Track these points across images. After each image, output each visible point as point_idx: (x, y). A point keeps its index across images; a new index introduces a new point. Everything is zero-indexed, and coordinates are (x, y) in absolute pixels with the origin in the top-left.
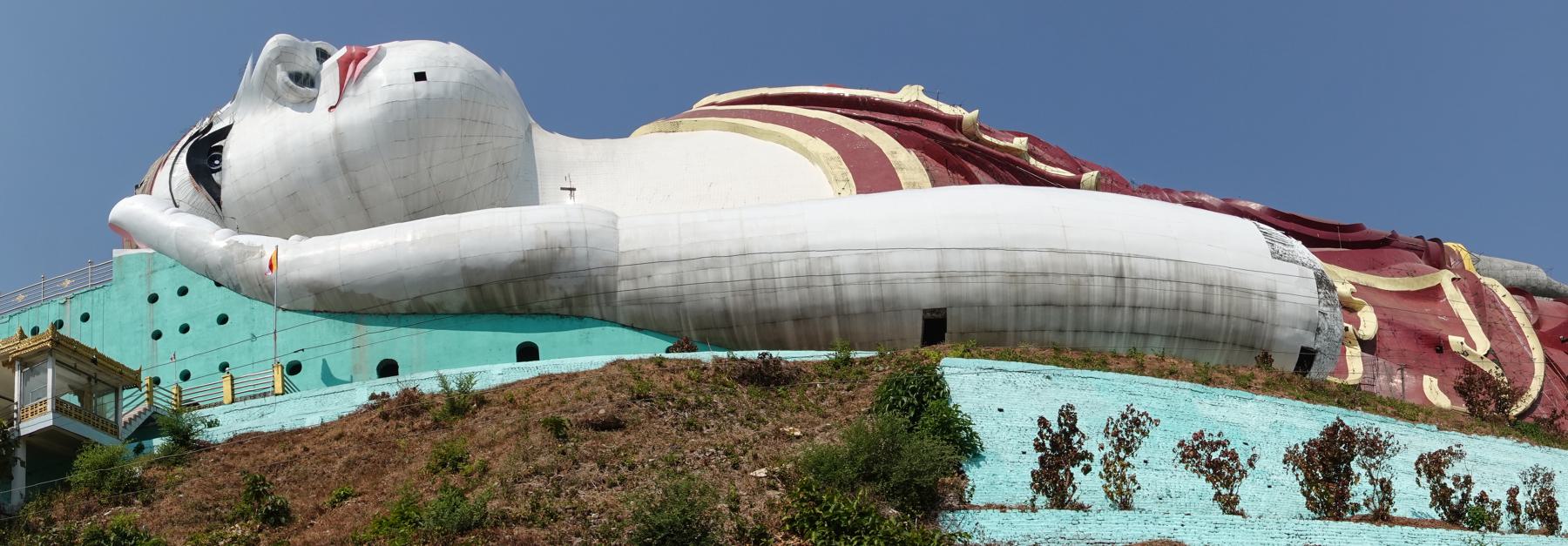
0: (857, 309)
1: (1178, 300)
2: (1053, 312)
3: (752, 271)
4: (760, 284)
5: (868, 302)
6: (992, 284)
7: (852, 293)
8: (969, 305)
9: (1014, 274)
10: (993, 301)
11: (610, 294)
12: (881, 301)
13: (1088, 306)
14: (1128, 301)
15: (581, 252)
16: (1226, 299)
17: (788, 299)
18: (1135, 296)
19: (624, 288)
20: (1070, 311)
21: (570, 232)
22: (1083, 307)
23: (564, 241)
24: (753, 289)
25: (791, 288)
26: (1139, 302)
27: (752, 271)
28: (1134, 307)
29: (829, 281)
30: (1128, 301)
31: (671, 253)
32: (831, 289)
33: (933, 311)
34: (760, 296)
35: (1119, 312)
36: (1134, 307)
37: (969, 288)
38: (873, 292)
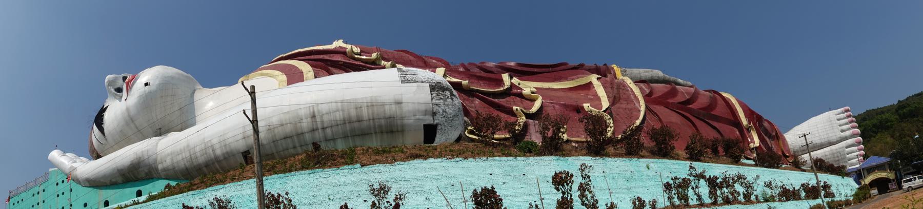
0: (222, 158)
1: (344, 120)
2: (289, 140)
11: (157, 169)
13: (302, 133)
14: (320, 126)
16: (370, 112)
17: (201, 160)
18: (322, 122)
19: (160, 167)
20: (295, 138)
22: (300, 134)
26: (325, 125)
28: (323, 129)
30: (320, 126)
35: (317, 133)
36: (323, 129)
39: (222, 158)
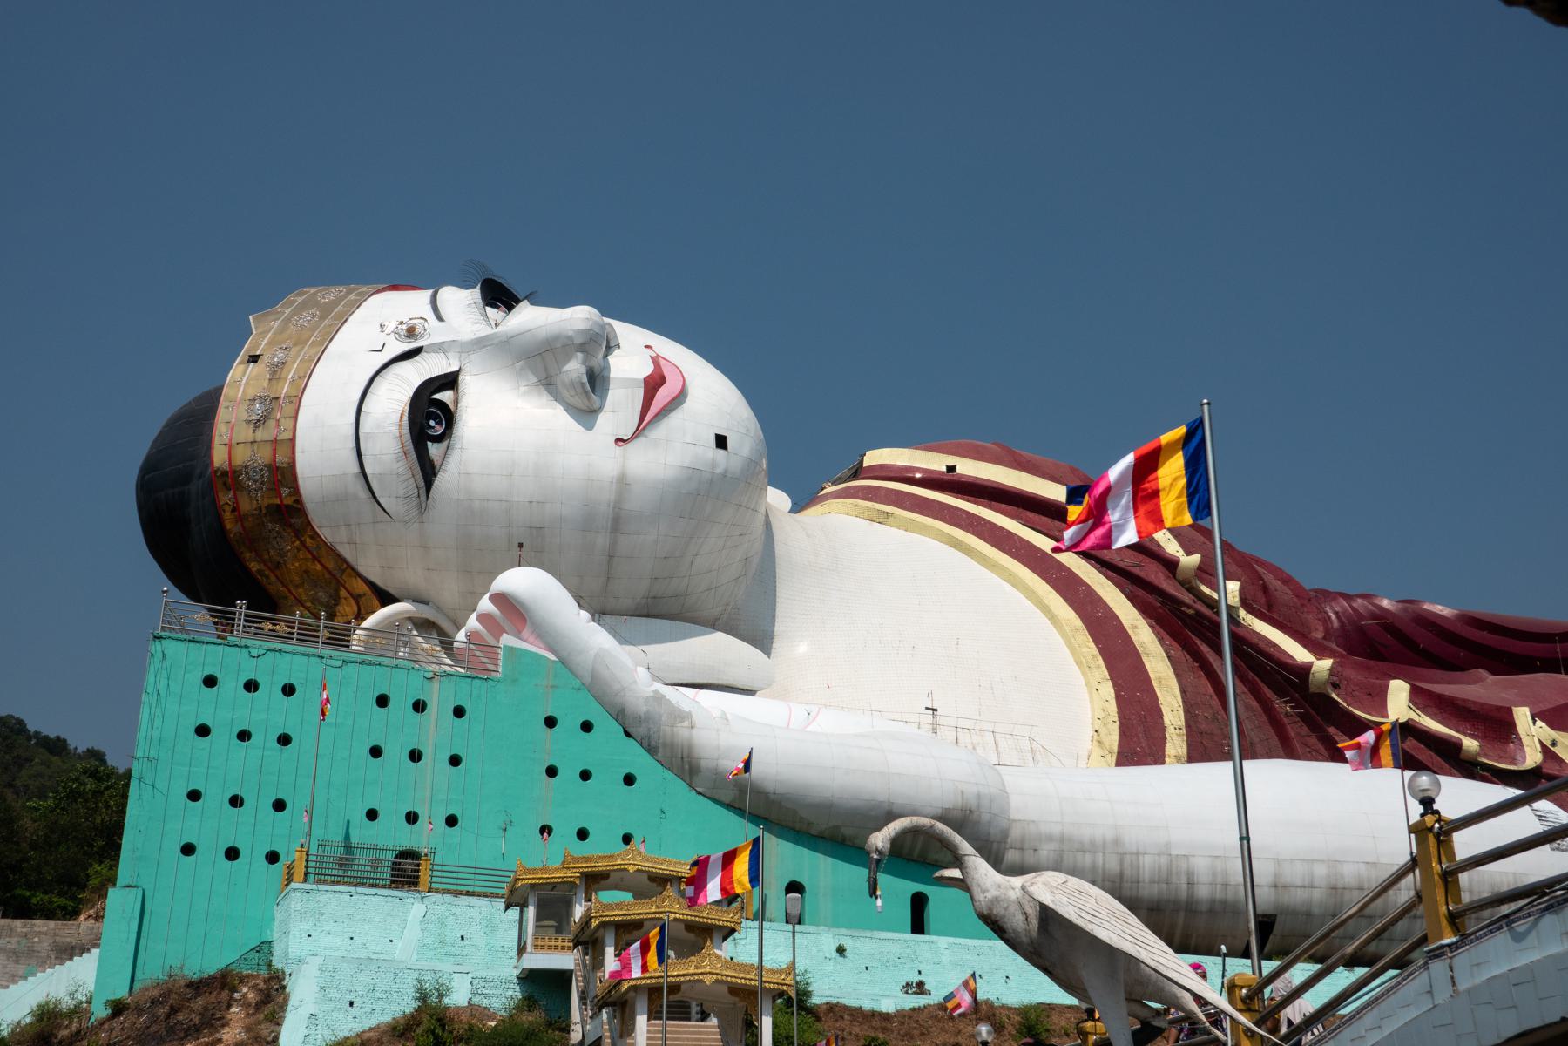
3: (1122, 864)
4: (1128, 872)
5: (1213, 902)
6: (1317, 895)
7: (1203, 892)
8: (1293, 912)
9: (1334, 888)
10: (1316, 911)
12: (1224, 903)
15: (985, 817)
21: (979, 796)
23: (973, 803)
24: (1121, 875)
25: (1152, 882)
27: (1122, 864)
29: (1184, 880)
31: (1056, 830)
32: (1185, 886)
33: (1265, 916)
34: (1126, 885)
37: (1298, 897)
38: (1219, 895)
39: (1204, 908)
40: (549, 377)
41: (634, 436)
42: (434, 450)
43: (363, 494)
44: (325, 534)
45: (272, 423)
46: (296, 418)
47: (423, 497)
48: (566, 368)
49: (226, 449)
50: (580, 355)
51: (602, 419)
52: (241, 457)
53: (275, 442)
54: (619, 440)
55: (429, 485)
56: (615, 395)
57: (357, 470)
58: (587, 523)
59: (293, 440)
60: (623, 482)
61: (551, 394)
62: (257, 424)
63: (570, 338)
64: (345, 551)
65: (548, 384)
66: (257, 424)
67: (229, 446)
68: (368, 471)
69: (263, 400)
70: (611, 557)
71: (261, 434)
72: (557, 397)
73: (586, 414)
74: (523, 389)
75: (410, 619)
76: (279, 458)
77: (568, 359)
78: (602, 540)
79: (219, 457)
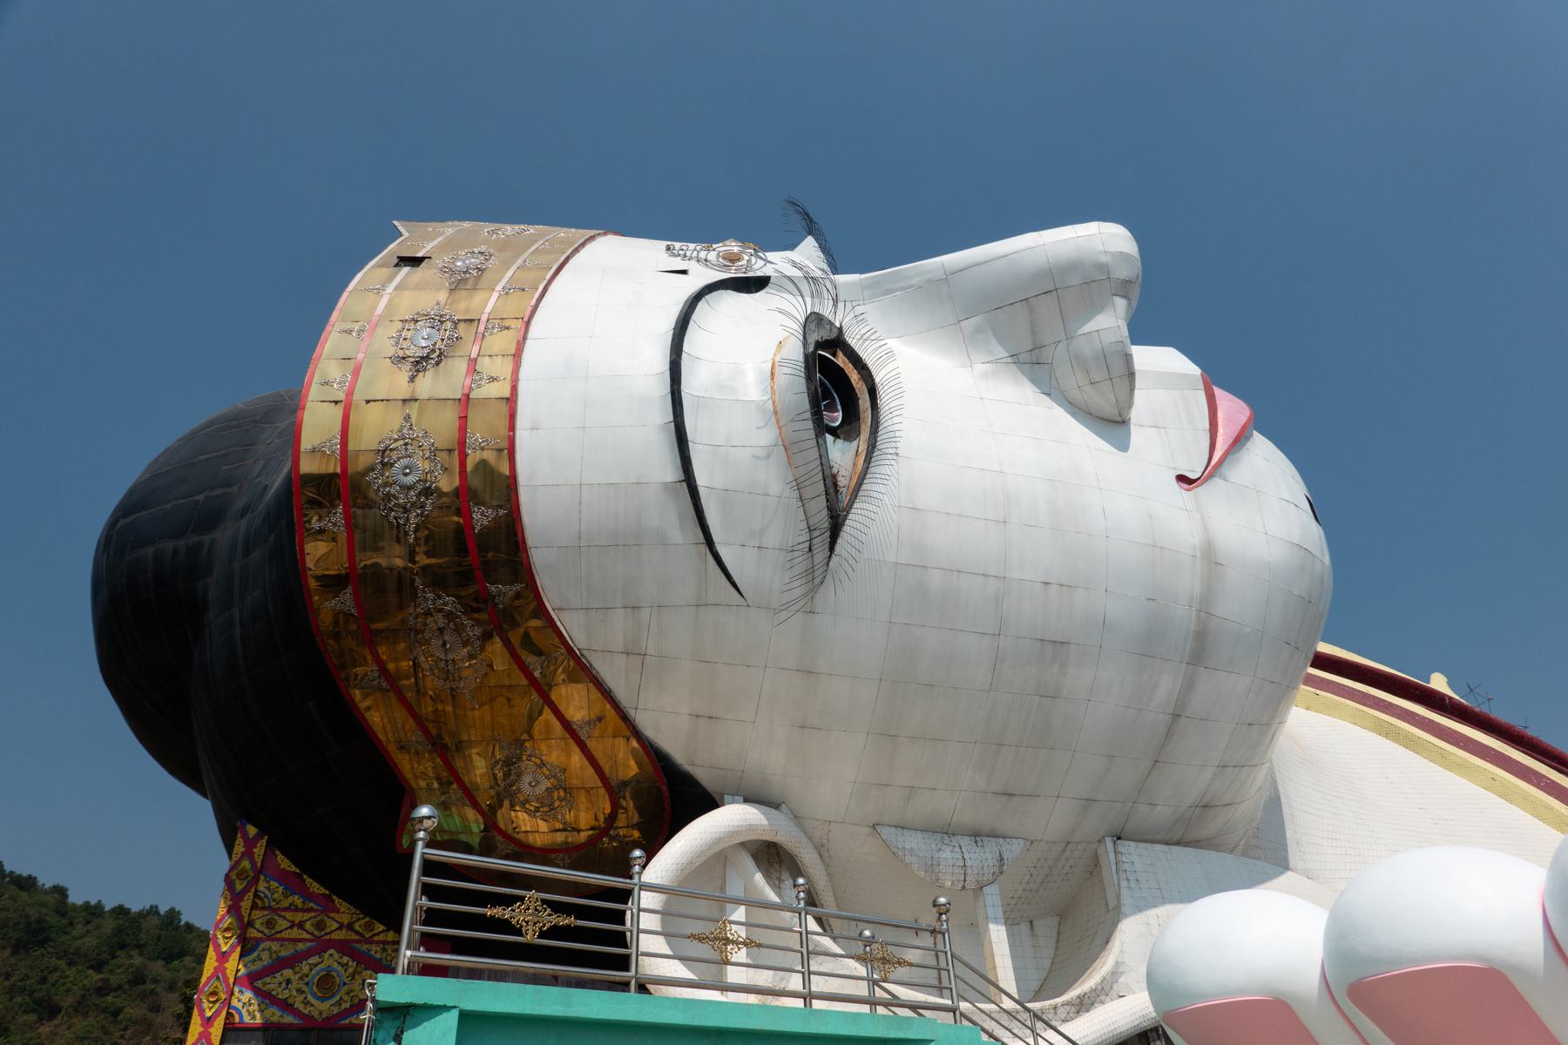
40: (1037, 347)
41: (1212, 470)
42: (841, 454)
43: (680, 532)
44: (573, 626)
45: (458, 367)
46: (517, 356)
47: (820, 557)
48: (1090, 327)
49: (338, 412)
50: (1120, 303)
51: (1137, 435)
52: (373, 428)
53: (465, 401)
54: (1182, 479)
55: (836, 526)
56: (1144, 403)
57: (672, 473)
58: (1149, 642)
59: (511, 400)
60: (1210, 557)
61: (1035, 381)
62: (419, 364)
63: (1102, 267)
64: (612, 673)
65: (1033, 362)
66: (419, 364)
67: (347, 407)
68: (701, 479)
69: (438, 320)
70: (1176, 716)
71: (427, 384)
72: (1051, 388)
73: (1112, 423)
74: (980, 368)
75: (743, 845)
76: (476, 435)
77: (1094, 307)
78: (1167, 684)
79: (318, 425)
